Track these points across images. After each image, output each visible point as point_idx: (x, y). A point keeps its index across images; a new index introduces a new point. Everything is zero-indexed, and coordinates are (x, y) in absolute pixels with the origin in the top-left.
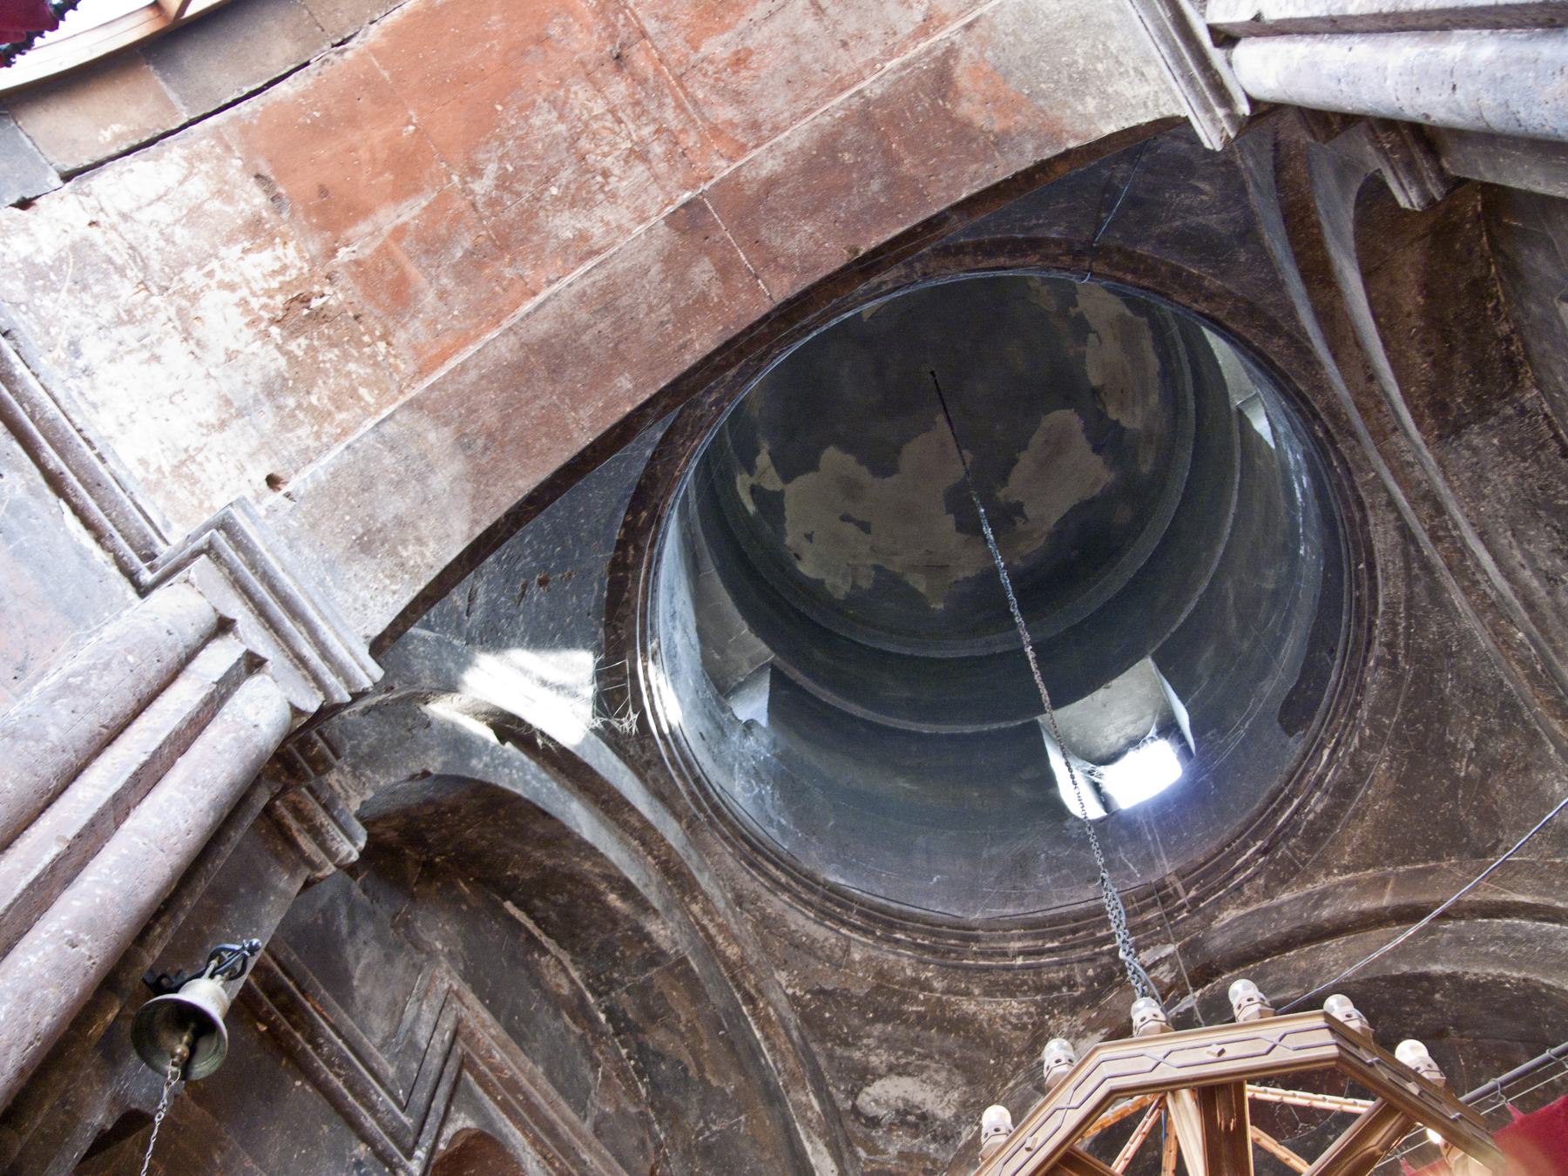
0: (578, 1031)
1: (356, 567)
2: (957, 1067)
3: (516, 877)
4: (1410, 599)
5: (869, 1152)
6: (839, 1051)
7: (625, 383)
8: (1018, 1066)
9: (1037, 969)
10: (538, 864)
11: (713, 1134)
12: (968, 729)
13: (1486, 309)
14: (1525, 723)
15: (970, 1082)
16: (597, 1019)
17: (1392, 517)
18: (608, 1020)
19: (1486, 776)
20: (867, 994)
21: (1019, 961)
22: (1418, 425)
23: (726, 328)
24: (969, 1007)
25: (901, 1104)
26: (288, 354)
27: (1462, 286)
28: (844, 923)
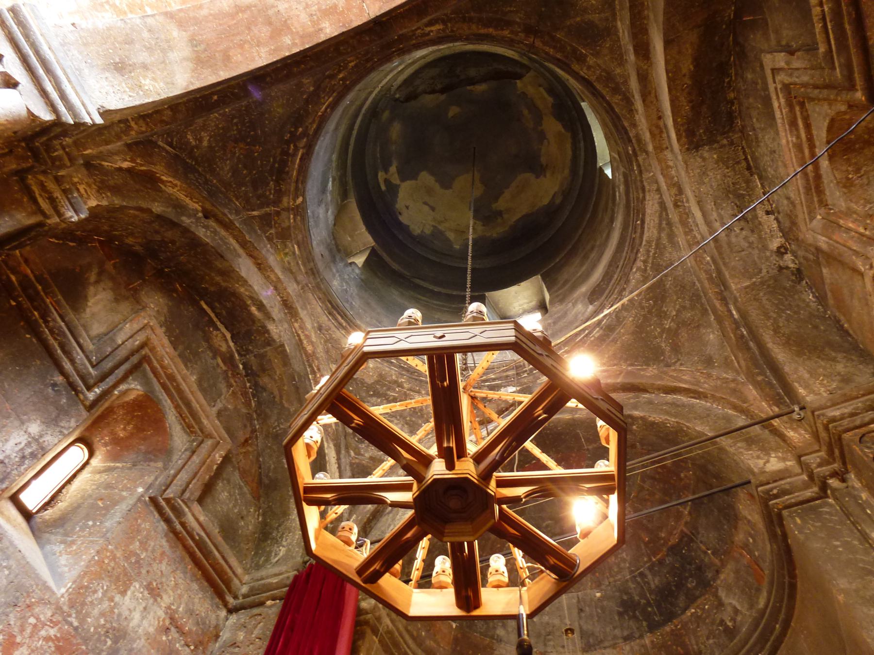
0: (224, 368)
1: (107, 74)
2: (407, 424)
3: (206, 288)
4: (659, 239)
5: (355, 454)
7: (287, 40)
10: (218, 284)
11: (281, 429)
12: (455, 293)
13: (724, 82)
14: (702, 305)
16: (238, 367)
17: (657, 197)
18: (244, 368)
19: (678, 328)
22: (678, 140)
23: (344, 25)
27: (714, 65)
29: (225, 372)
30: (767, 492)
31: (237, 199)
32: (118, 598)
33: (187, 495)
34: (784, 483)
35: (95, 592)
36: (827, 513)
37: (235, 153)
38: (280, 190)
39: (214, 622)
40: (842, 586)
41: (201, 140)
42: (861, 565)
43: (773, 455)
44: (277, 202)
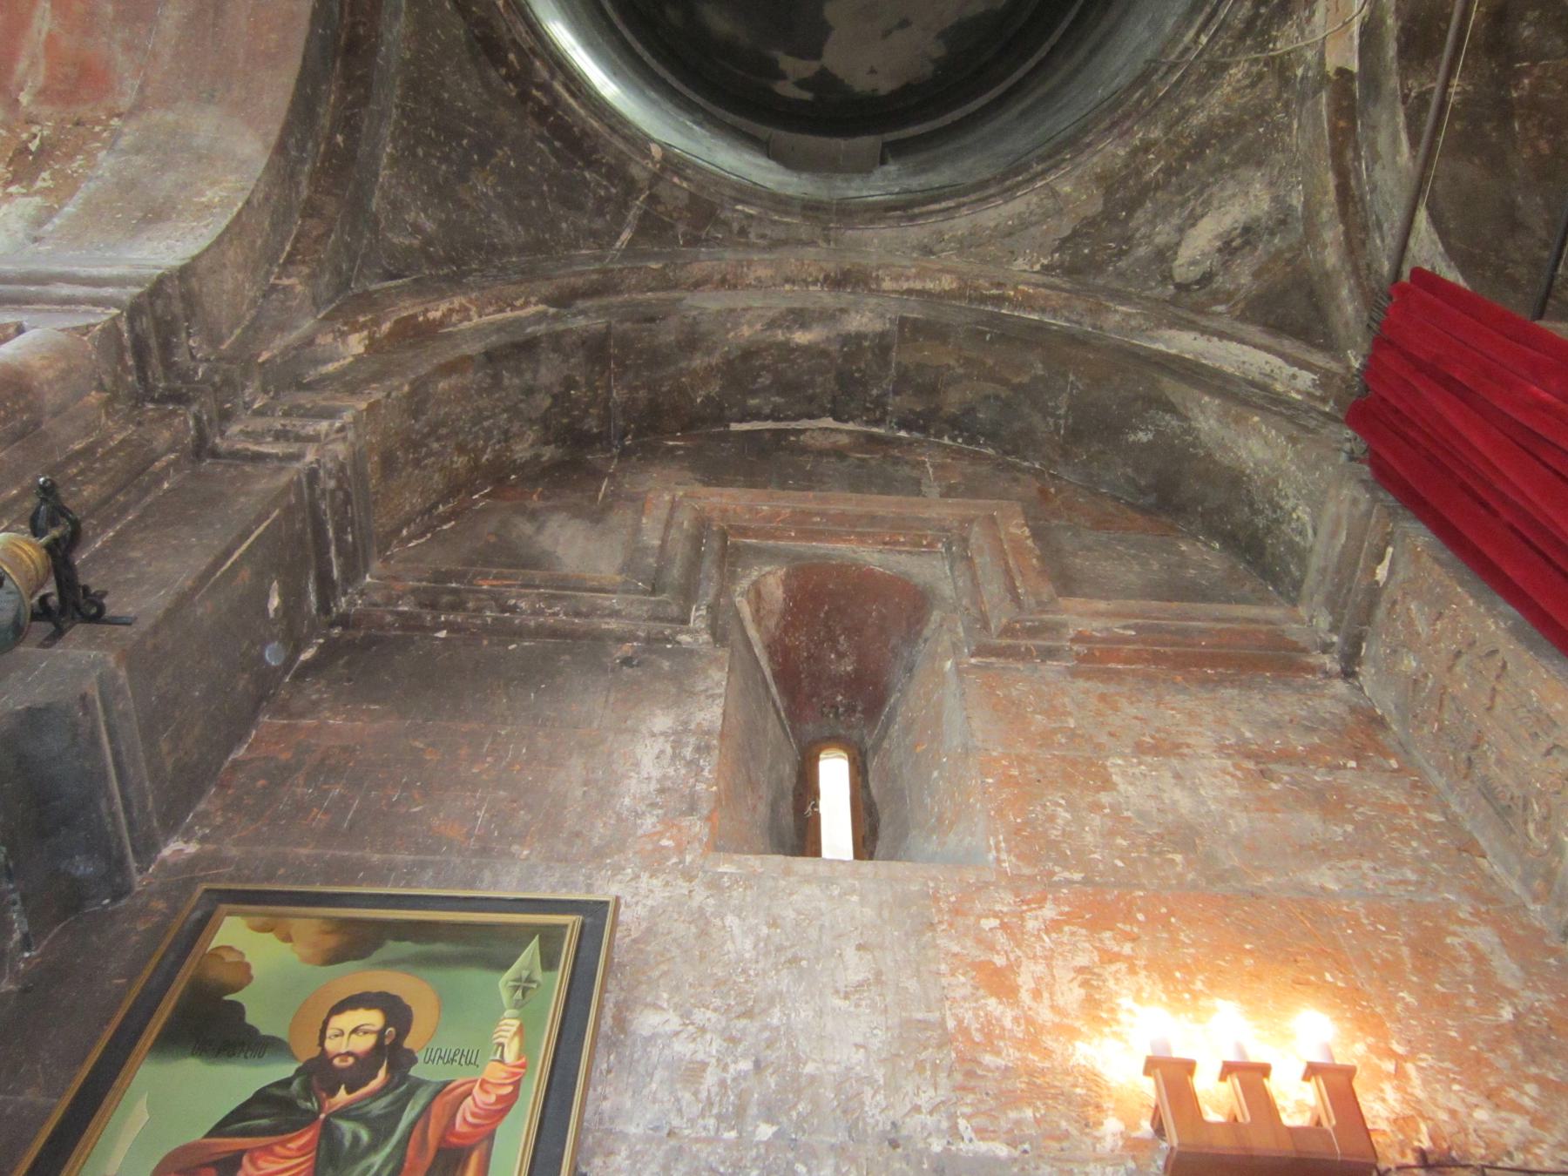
2: (1234, 167)
3: (708, 398)
6: (1122, 264)
8: (1287, 105)
9: (1223, 25)
10: (710, 370)
11: (1066, 418)
15: (1259, 164)
16: (900, 438)
20: (1105, 204)
21: (1204, 39)
24: (1199, 119)
25: (1218, 244)
26: (40, 192)
28: (1032, 180)
29: (884, 457)
31: (577, 247)
32: (1105, 798)
33: (1029, 601)
35: (1052, 818)
37: (485, 195)
38: (610, 167)
39: (1340, 709)
41: (417, 229)
44: (631, 187)
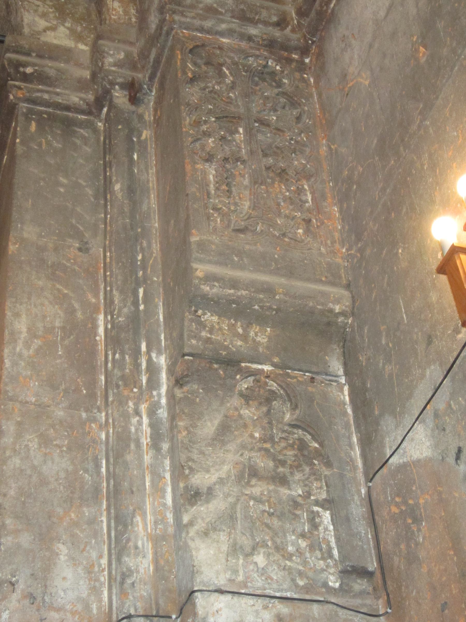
30: (19, 64)
34: (50, 67)
36: (84, 137)
40: (26, 235)
42: (74, 221)
43: (68, 25)
